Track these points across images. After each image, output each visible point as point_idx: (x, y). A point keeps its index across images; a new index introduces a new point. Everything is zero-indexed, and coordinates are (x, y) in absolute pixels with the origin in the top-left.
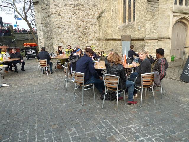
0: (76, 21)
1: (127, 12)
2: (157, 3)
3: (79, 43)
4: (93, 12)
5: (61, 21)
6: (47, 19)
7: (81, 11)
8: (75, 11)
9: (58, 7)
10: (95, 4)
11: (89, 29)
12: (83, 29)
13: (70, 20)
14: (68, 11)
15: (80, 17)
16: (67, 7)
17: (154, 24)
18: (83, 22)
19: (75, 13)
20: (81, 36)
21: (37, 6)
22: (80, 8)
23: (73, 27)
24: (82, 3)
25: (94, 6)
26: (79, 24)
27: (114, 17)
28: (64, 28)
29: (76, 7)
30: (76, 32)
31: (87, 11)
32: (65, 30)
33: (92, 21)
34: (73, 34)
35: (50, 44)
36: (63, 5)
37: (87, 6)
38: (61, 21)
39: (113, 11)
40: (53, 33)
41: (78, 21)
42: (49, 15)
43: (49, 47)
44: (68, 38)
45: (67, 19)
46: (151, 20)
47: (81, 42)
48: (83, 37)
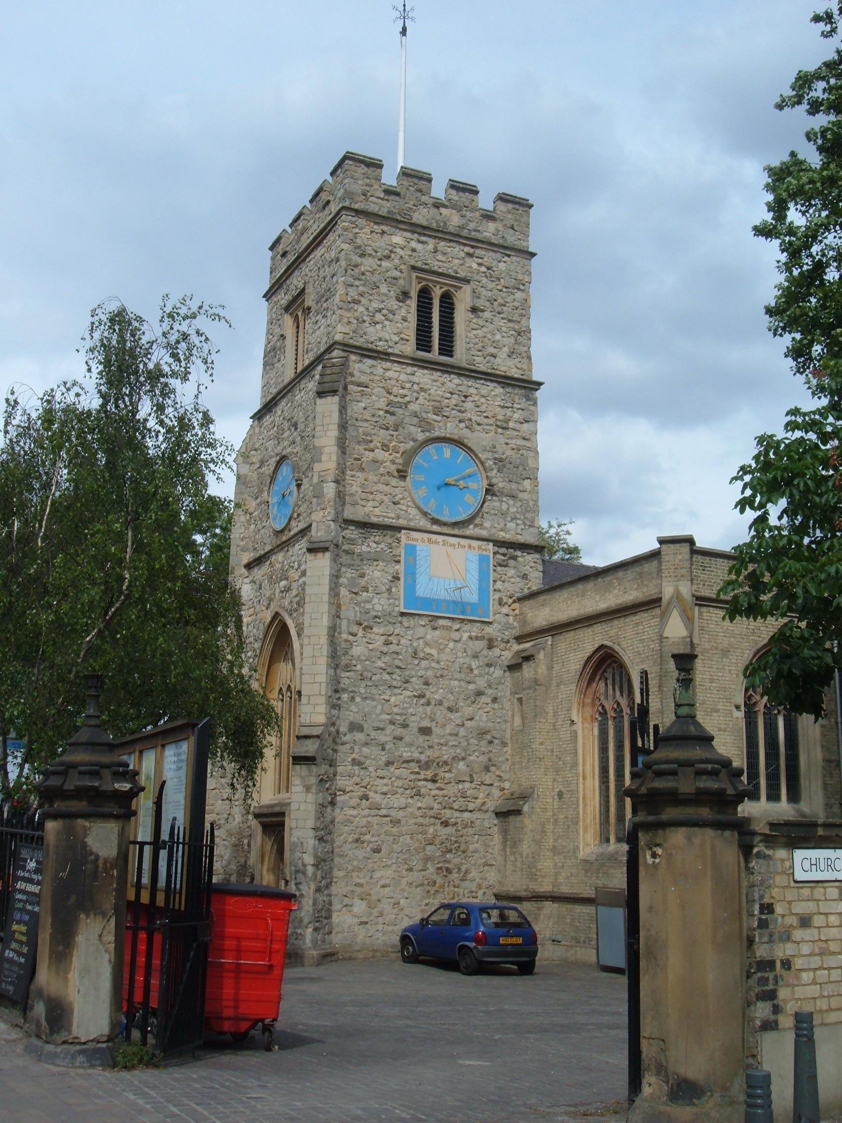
0: (420, 820)
3: (427, 904)
4: (483, 788)
7: (442, 786)
10: (490, 760)
11: (464, 852)
12: (444, 853)
14: (395, 784)
15: (436, 806)
16: (392, 769)
18: (446, 824)
19: (418, 794)
20: (435, 877)
21: (304, 768)
22: (436, 775)
24: (445, 757)
25: (487, 769)
26: (431, 830)
27: (566, 817)
28: (374, 845)
30: (416, 862)
31: (460, 787)
32: (377, 851)
33: (478, 822)
34: (407, 870)
35: (324, 901)
37: (461, 765)
38: (369, 819)
39: (560, 795)
40: (337, 860)
41: (427, 821)
44: (388, 881)
47: (431, 901)
48: (439, 881)
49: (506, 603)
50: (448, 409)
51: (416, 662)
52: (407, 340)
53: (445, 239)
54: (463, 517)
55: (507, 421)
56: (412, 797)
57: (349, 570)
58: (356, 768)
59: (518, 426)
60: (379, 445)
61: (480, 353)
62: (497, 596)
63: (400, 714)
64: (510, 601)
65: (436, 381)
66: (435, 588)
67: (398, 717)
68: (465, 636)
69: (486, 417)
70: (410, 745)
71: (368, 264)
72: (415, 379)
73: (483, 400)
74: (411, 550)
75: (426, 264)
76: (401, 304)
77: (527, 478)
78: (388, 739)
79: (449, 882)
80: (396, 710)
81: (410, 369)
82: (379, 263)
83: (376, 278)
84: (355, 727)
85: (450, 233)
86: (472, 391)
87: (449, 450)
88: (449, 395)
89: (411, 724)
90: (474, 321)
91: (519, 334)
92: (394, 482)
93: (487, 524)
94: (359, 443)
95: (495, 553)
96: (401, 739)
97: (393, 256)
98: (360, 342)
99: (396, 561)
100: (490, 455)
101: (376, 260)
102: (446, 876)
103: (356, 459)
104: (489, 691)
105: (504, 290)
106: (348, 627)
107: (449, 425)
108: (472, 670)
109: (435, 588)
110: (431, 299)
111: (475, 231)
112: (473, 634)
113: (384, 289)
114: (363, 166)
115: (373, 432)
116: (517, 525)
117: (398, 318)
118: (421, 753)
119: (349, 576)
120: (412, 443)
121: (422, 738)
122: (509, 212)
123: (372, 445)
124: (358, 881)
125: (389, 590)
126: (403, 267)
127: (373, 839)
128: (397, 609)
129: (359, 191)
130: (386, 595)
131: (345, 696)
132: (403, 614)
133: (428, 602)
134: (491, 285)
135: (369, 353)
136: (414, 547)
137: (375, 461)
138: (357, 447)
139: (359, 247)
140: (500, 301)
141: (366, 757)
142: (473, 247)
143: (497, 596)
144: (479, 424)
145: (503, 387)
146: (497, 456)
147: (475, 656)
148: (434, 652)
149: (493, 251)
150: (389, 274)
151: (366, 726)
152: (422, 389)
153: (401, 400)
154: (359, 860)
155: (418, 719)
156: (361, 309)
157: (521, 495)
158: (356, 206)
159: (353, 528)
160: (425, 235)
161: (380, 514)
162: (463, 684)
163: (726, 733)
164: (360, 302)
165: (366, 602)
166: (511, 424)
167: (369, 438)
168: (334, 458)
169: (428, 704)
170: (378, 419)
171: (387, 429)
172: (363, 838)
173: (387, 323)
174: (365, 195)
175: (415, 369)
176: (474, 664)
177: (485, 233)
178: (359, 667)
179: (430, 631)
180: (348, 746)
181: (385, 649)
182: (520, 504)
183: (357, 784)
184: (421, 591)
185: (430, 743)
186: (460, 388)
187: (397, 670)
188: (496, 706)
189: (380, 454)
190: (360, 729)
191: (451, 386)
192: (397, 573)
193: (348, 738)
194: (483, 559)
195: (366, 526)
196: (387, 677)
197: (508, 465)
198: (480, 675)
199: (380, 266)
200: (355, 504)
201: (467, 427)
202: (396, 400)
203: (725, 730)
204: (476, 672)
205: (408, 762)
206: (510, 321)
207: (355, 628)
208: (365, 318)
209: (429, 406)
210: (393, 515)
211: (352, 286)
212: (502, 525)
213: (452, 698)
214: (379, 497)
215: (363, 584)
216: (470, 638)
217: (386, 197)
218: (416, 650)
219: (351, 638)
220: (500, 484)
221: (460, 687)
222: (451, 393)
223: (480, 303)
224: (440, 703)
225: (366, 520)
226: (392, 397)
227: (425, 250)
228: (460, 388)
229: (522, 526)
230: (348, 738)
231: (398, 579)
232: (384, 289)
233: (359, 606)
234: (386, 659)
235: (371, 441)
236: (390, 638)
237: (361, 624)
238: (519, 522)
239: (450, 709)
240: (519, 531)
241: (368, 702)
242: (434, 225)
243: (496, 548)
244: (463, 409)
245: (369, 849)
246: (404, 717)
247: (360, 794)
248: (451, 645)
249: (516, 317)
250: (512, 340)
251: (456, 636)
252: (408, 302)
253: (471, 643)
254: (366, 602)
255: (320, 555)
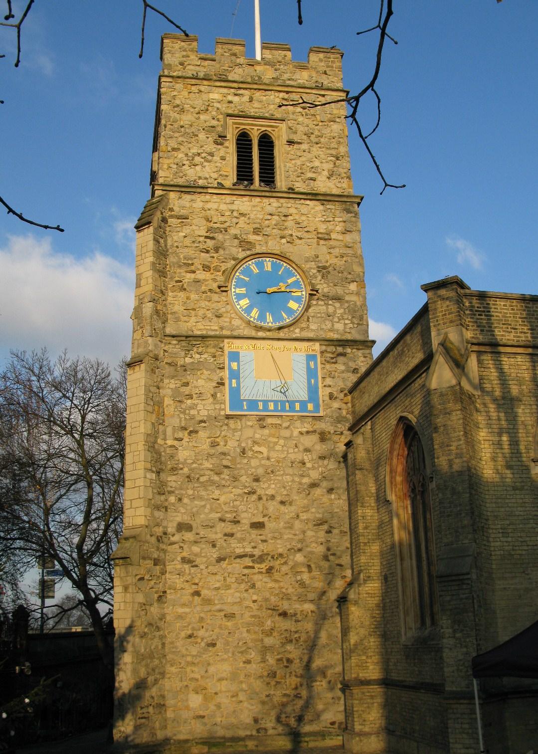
1: (426, 589)
2: (465, 587)
5: (202, 615)
6: (152, 609)
8: (256, 577)
9: (195, 568)
10: (328, 549)
13: (235, 609)
14: (228, 579)
17: (465, 650)
23: (245, 635)
24: (280, 551)
28: (209, 640)
29: (257, 566)
30: (253, 655)
34: (244, 662)
36: (213, 560)
37: (299, 557)
40: (170, 657)
42: (160, 596)
43: (151, 709)
45: (224, 607)
46: (454, 637)
49: (336, 398)
50: (268, 229)
51: (245, 461)
52: (227, 176)
53: (260, 90)
54: (288, 321)
55: (328, 234)
56: (246, 591)
57: (172, 381)
58: (186, 566)
59: (340, 237)
60: (200, 267)
61: (300, 178)
62: (328, 390)
63: (231, 512)
64: (342, 395)
65: (254, 206)
66: (261, 391)
67: (228, 515)
68: (296, 433)
69: (308, 232)
70: (242, 540)
71: (186, 119)
72: (234, 207)
73: (304, 218)
74: (235, 357)
75: (242, 112)
76: (219, 147)
77: (353, 281)
78: (220, 535)
79: (291, 673)
80: (226, 508)
81: (228, 199)
82: (197, 116)
83: (193, 129)
84: (183, 527)
85: (265, 84)
86: (293, 211)
87: (269, 264)
88: (269, 217)
89: (243, 521)
90: (292, 153)
91: (338, 159)
92: (215, 297)
93: (313, 327)
94: (180, 266)
95: (322, 352)
96: (232, 535)
97: (210, 108)
98: (181, 181)
99: (220, 368)
100: (313, 264)
101: (195, 115)
102: (287, 667)
103: (177, 282)
104: (325, 484)
105: (320, 124)
106: (173, 434)
107: (270, 243)
108: (304, 464)
109: (261, 391)
110: (251, 141)
111: (289, 80)
112: (305, 430)
113: (202, 136)
114: (179, 42)
115: (193, 256)
116: (345, 324)
117: (216, 158)
118: (254, 547)
119: (172, 386)
120: (233, 262)
121: (254, 532)
122: (321, 60)
123: (193, 268)
124: (192, 675)
125: (214, 396)
126: (221, 117)
127: (207, 634)
128: (222, 413)
129: (177, 63)
130: (211, 400)
131: (172, 499)
132: (228, 417)
133: (253, 404)
134: (306, 121)
135: (189, 188)
136: (238, 353)
137: (197, 281)
138: (178, 271)
139: (178, 106)
140: (316, 133)
141: (196, 555)
142: (287, 92)
143: (328, 390)
144: (301, 239)
145: (323, 205)
146: (320, 265)
147: (307, 450)
148: (263, 449)
149: (307, 93)
150: (208, 124)
151: (194, 525)
152: (241, 214)
153: (222, 226)
154: (193, 656)
155: (250, 515)
156: (181, 155)
157: (347, 298)
158: (175, 74)
159: (175, 342)
160: (240, 88)
161: (203, 327)
162: (297, 479)
163: (523, 492)
164: (179, 149)
165: (191, 408)
166: (333, 236)
167: (190, 262)
168: (150, 280)
169: (260, 498)
170: (198, 245)
171: (208, 252)
172: (195, 633)
173: (206, 164)
174: (182, 64)
175: (234, 198)
176: (307, 457)
177: (299, 81)
178: (186, 470)
179: (260, 431)
180: (176, 546)
181: (212, 451)
182: (347, 305)
183: (187, 581)
184: (246, 394)
185: (263, 538)
186: (279, 210)
187: (226, 470)
188: (333, 496)
189: (201, 275)
190: (189, 528)
191: (269, 209)
192: (222, 379)
193: (176, 538)
194: (311, 358)
195: (189, 340)
196: (216, 478)
197: (332, 272)
198: (313, 468)
199: (198, 118)
200: (178, 320)
201: (288, 242)
202: (216, 226)
203: (522, 489)
204: (309, 465)
205: (240, 557)
206: (329, 149)
207: (180, 435)
208: (185, 162)
209: (250, 228)
210: (216, 328)
211: (171, 137)
212: (329, 325)
213: (285, 493)
214: (201, 312)
215: (187, 393)
216: (301, 433)
217: (202, 64)
218: (244, 449)
219: (176, 443)
220: (323, 288)
221: (293, 481)
222: (271, 214)
223: (296, 138)
224: (273, 497)
225: (190, 333)
226: (212, 225)
227: (240, 101)
228: (279, 210)
229: (351, 325)
230: (176, 538)
231: (223, 384)
232: (202, 136)
233: (184, 413)
234: (214, 460)
235: (192, 264)
236: (217, 440)
237: (186, 429)
238: (347, 322)
239: (282, 503)
240: (348, 330)
241: (196, 502)
242: (249, 80)
243: (324, 348)
244: (284, 227)
245: (203, 644)
246: (235, 515)
247: (191, 591)
248: (282, 442)
249: (333, 145)
250: (331, 165)
251: (286, 433)
252: (227, 144)
253: (302, 438)
254: (191, 408)
255: (137, 368)
